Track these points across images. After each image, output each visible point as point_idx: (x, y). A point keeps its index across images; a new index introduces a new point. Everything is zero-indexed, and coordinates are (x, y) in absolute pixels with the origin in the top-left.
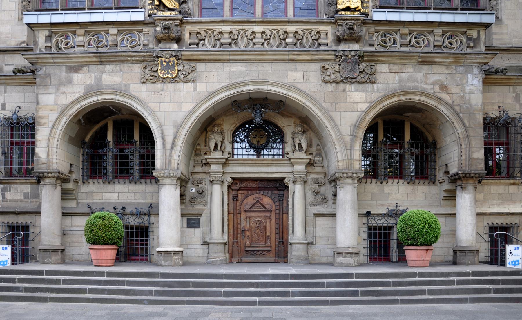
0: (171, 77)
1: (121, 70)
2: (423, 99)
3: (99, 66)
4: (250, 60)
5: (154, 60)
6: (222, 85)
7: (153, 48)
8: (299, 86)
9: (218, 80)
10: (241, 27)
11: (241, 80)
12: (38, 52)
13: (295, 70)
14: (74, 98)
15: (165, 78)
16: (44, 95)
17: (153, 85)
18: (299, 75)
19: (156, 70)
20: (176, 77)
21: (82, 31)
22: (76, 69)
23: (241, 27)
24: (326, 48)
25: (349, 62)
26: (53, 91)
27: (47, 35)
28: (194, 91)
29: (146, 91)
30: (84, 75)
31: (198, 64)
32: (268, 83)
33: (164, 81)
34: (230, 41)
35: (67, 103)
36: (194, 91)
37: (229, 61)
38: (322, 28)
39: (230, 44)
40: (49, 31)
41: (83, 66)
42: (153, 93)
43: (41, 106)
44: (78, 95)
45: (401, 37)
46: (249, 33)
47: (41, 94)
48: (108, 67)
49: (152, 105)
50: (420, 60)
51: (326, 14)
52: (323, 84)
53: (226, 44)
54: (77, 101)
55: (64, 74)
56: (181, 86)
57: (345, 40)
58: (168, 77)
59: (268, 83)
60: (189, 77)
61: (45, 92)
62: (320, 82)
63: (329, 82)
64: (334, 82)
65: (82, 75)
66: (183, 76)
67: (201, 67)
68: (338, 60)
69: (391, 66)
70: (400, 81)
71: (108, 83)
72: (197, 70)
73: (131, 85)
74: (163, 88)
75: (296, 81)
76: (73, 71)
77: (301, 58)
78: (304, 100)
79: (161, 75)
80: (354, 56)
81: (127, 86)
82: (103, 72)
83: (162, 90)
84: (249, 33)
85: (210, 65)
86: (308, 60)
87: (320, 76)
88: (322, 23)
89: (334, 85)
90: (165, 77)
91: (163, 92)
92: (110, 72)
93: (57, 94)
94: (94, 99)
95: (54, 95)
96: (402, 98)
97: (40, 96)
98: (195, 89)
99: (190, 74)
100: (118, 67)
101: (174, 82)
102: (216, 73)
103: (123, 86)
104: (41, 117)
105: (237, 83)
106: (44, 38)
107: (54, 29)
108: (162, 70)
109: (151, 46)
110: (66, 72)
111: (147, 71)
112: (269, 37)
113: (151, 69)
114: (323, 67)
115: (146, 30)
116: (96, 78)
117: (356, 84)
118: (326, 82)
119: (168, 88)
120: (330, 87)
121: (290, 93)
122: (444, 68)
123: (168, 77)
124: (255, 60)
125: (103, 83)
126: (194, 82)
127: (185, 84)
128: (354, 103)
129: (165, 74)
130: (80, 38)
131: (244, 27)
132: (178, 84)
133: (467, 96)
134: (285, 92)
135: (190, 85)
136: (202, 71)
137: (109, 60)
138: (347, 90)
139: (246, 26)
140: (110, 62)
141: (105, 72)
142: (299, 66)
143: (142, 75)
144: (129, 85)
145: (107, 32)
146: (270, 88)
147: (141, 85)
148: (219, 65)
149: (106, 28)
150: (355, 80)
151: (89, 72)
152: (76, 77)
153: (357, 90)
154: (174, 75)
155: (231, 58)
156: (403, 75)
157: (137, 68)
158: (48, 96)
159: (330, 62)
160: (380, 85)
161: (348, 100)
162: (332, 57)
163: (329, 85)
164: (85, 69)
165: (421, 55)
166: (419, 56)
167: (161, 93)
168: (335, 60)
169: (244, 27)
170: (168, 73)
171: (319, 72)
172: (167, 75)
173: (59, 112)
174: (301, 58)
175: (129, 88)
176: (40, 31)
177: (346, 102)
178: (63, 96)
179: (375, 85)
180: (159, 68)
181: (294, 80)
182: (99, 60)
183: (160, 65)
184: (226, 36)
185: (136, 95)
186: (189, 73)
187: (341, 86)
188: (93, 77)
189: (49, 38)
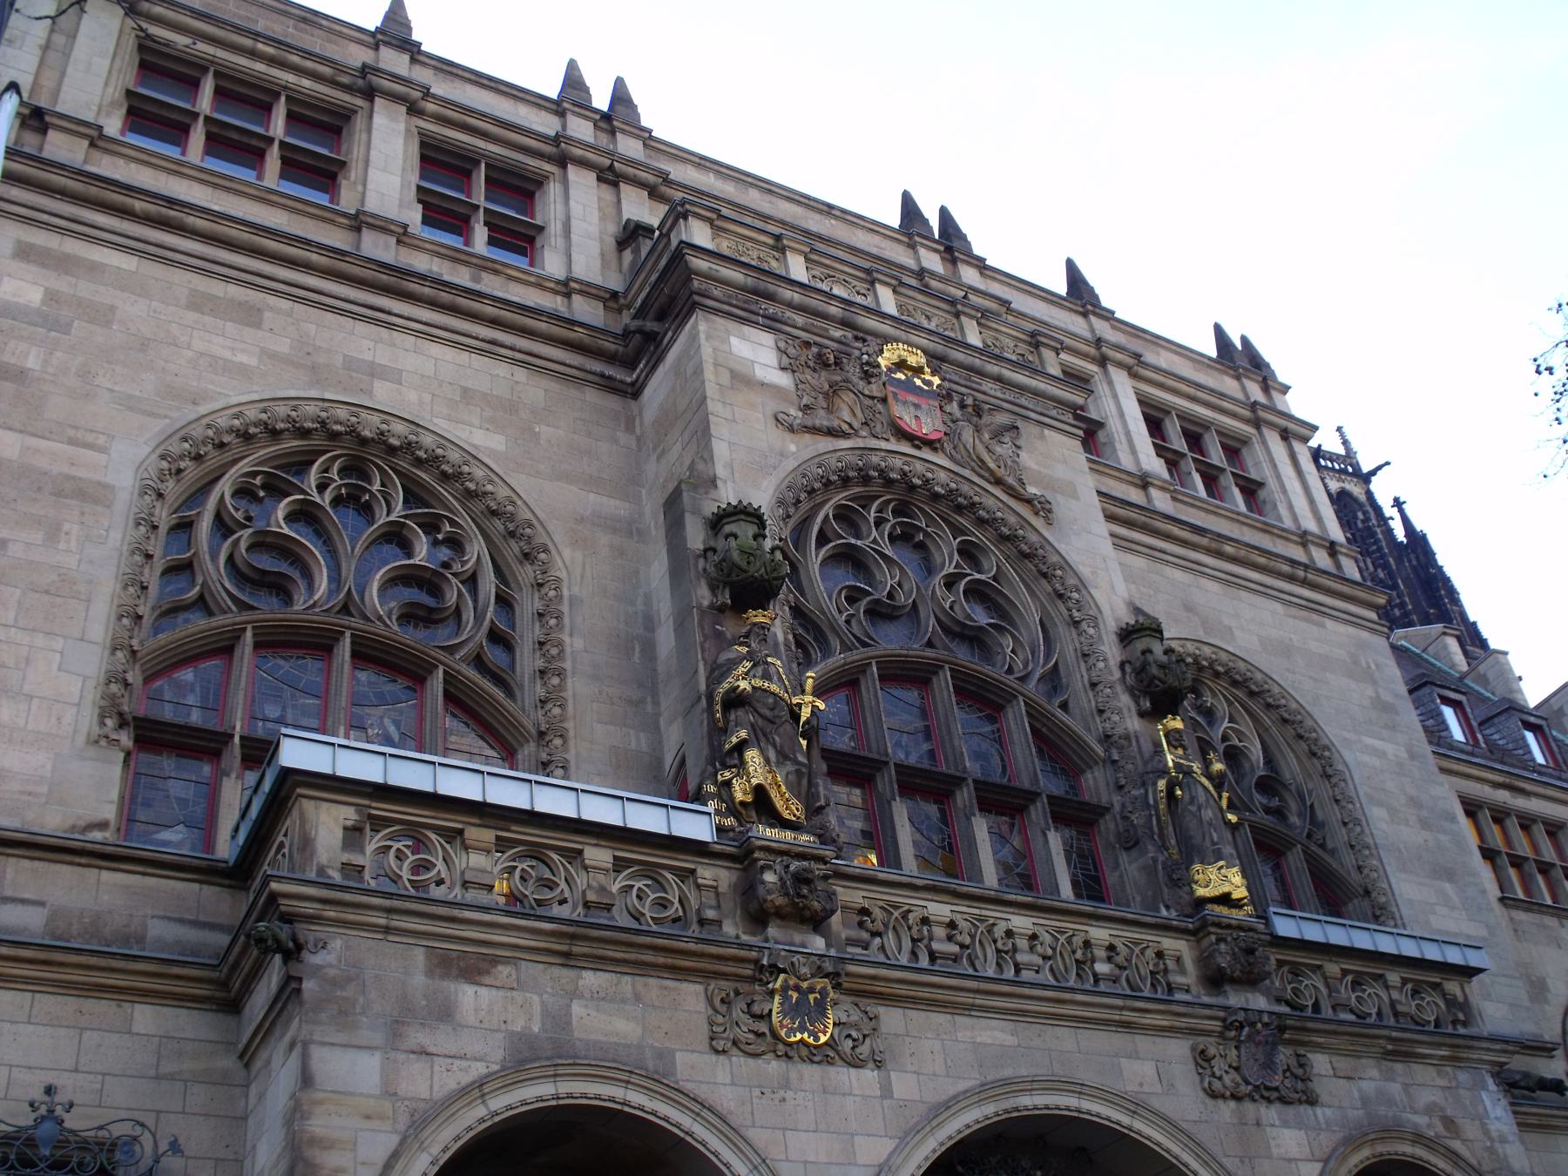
0: (811, 1040)
1: (638, 998)
2: (1420, 1152)
3: (556, 971)
4: (1024, 1013)
5: (752, 980)
6: (962, 1085)
7: (737, 937)
8: (1155, 1103)
9: (947, 1067)
10: (977, 911)
11: (1008, 1072)
12: (312, 876)
13: (1134, 1055)
14: (466, 1079)
15: (790, 1045)
16: (338, 1052)
17: (751, 1061)
18: (1148, 1069)
19: (766, 1011)
20: (826, 1043)
21: (488, 836)
22: (474, 970)
23: (977, 911)
24: (1187, 997)
25: (1258, 1044)
26: (378, 1038)
27: (349, 823)
28: (883, 1097)
29: (733, 1084)
30: (501, 993)
31: (881, 1009)
32: (1080, 1089)
33: (789, 1052)
34: (955, 949)
35: (438, 1094)
36: (883, 1097)
37: (967, 1009)
38: (1170, 944)
39: (956, 959)
40: (358, 812)
41: (495, 961)
42: (757, 1092)
43: (321, 1095)
44: (479, 1069)
45: (1327, 986)
46: (999, 931)
47: (324, 1044)
48: (591, 979)
49: (758, 1136)
50: (1390, 1047)
51: (1167, 907)
52: (1209, 1101)
53: (945, 956)
54: (479, 1088)
55: (419, 980)
56: (842, 1075)
57: (1234, 981)
58: (802, 1040)
59: (1080, 1089)
60: (864, 1050)
61: (341, 1038)
62: (1202, 1094)
63: (1223, 1097)
64: (1234, 1097)
65: (494, 992)
66: (850, 1043)
67: (892, 1019)
68: (1233, 1033)
69: (1335, 1059)
70: (1365, 1101)
71: (592, 1037)
72: (884, 1029)
73: (678, 1055)
74: (787, 1080)
75: (1146, 1089)
76: (455, 971)
77: (1148, 1020)
78: (1175, 1149)
79: (783, 1033)
80: (1266, 1025)
81: (665, 1055)
82: (575, 994)
83: (786, 1085)
84: (999, 931)
85: (917, 1017)
86: (1163, 1029)
87: (1197, 1078)
88: (1165, 928)
89: (1232, 1104)
90: (793, 1039)
91: (789, 1095)
92: (597, 998)
93: (392, 1055)
94: (537, 1092)
95: (378, 1055)
96: (1381, 1148)
97: (317, 1053)
98: (887, 1091)
99: (868, 1041)
100: (627, 983)
101: (818, 1063)
102: (937, 1043)
103: (648, 1054)
104: (328, 1145)
105: (1006, 1082)
106: (339, 833)
107: (381, 809)
108: (784, 1013)
109: (729, 929)
110: (429, 973)
111: (738, 1012)
112: (1050, 952)
113: (749, 1005)
114: (1203, 1052)
115: (708, 873)
116: (546, 1013)
117: (1278, 1105)
118: (1213, 1095)
119: (801, 1078)
120: (1227, 1109)
121: (1138, 1125)
122: (1431, 1070)
123: (802, 1040)
124: (1038, 1014)
125: (576, 1034)
126: (879, 1064)
127: (852, 1070)
128: (1290, 1160)
129: (792, 1031)
130: (477, 859)
131: (984, 912)
132: (831, 1069)
133: (1497, 1145)
134: (1125, 1120)
135: (869, 1075)
136: (897, 1035)
137: (601, 952)
138: (1264, 1122)
139: (991, 912)
140: (599, 963)
141: (582, 997)
142: (1143, 1042)
143: (711, 1023)
144: (672, 1052)
145: (575, 855)
146: (1086, 1105)
147: (714, 1057)
148: (940, 1019)
149: (571, 842)
150: (1276, 1094)
151: (520, 986)
152: (470, 998)
153: (1286, 1124)
154: (823, 1039)
155: (978, 1002)
156: (1364, 1085)
157: (692, 997)
158: (351, 1055)
159: (1212, 1040)
160: (1328, 1111)
161: (1275, 1151)
162: (1216, 1025)
163: (1220, 1102)
164: (504, 971)
165: (1394, 1034)
166: (1389, 1039)
167: (782, 1093)
168: (1221, 1035)
169: (984, 912)
170: (802, 1029)
171: (1192, 1066)
172: (799, 1036)
173: (401, 1127)
174: (1148, 1020)
175: (674, 1063)
176: (325, 805)
177: (1270, 1157)
178: (418, 1066)
179: (1319, 1111)
180: (776, 1007)
181: (1141, 1085)
182: (564, 948)
183: (777, 998)
184: (940, 932)
185: (703, 1092)
186: (865, 1036)
187: (1248, 1106)
188: (537, 1009)
189: (353, 835)
